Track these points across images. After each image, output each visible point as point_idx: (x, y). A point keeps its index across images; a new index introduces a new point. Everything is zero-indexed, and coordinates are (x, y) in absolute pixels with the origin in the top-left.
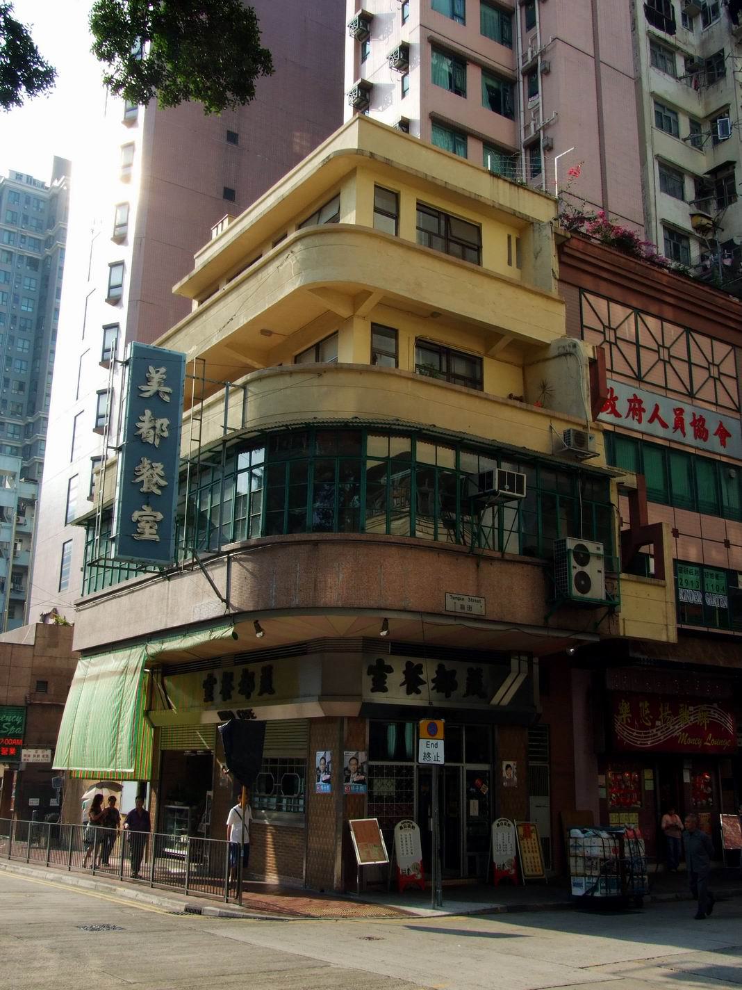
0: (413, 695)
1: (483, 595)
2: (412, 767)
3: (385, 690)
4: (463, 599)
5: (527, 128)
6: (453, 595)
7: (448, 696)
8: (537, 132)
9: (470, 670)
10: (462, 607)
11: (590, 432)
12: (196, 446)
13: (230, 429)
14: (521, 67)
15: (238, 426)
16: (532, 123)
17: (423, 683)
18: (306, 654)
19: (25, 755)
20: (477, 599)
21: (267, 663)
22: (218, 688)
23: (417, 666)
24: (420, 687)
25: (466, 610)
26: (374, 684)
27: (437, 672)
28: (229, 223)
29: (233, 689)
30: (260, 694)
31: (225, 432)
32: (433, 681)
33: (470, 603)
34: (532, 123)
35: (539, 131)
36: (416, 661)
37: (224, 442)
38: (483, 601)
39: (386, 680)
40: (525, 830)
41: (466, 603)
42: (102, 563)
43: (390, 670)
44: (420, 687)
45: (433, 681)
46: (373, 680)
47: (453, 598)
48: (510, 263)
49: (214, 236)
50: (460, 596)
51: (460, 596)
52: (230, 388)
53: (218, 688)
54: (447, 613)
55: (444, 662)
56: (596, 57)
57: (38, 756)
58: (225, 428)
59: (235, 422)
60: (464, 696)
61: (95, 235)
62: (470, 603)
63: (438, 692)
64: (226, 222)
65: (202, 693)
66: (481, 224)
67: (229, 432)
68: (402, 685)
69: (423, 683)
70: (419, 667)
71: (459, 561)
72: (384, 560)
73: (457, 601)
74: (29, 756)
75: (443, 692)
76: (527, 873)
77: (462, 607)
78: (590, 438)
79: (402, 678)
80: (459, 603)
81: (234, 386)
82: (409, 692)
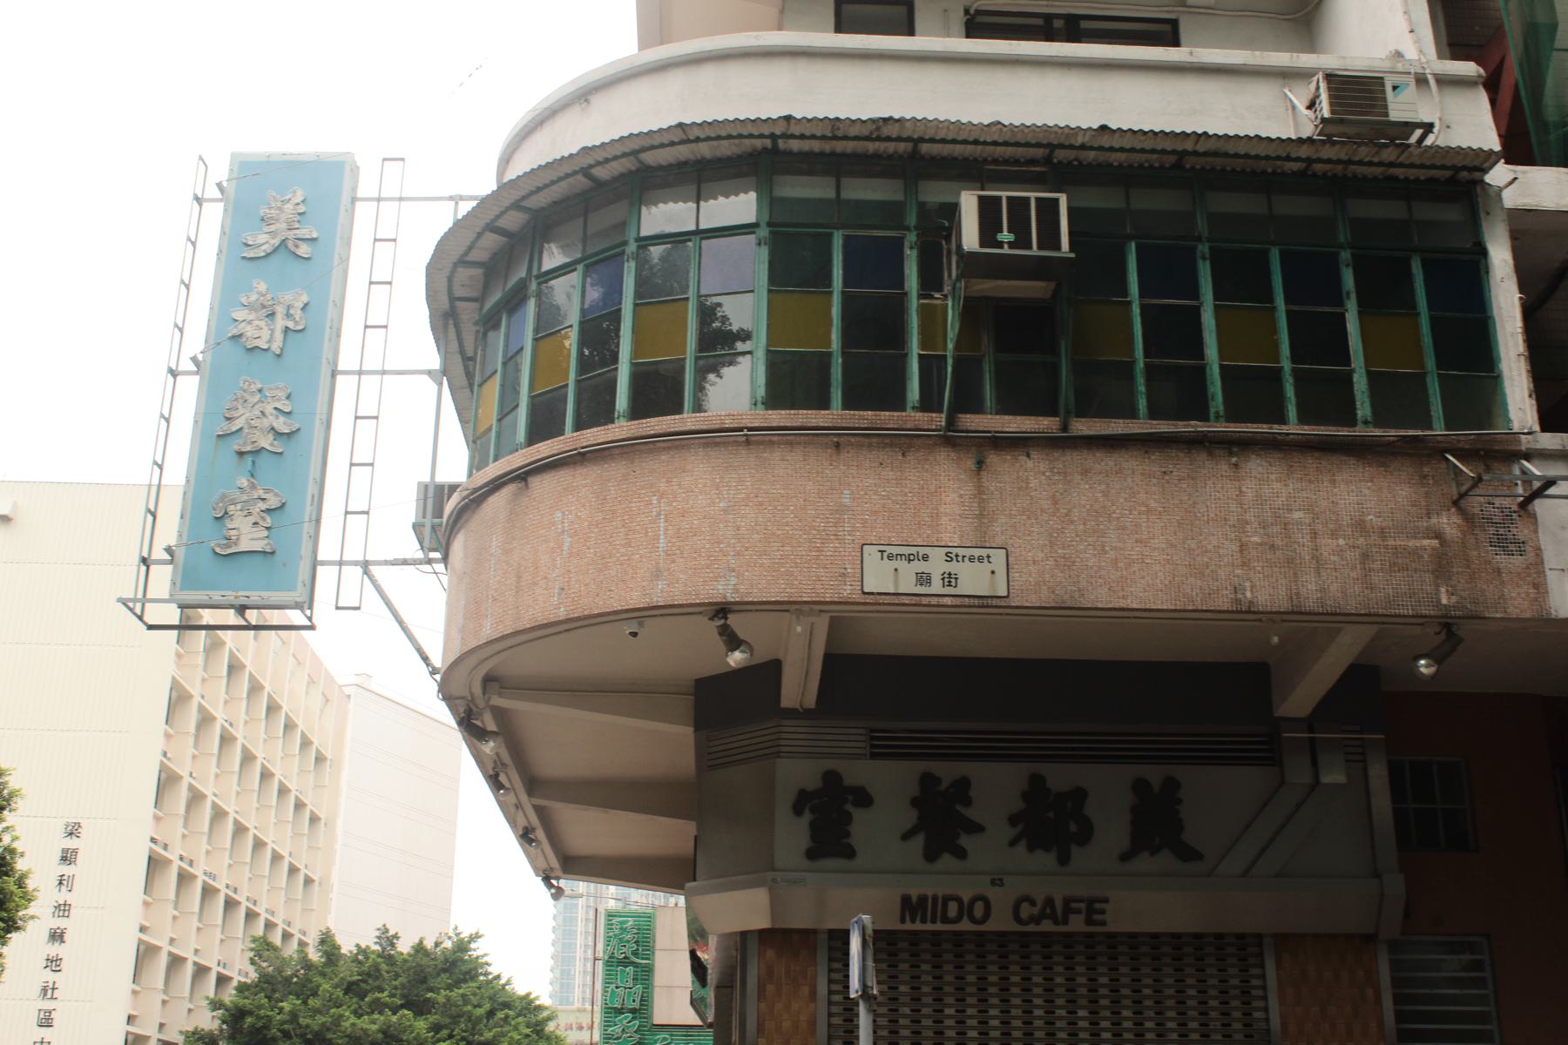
0: (947, 861)
1: (999, 541)
4: (925, 558)
6: (890, 549)
7: (1064, 859)
9: (1140, 786)
10: (924, 579)
17: (976, 828)
20: (977, 552)
24: (965, 841)
25: (936, 587)
26: (813, 837)
32: (1013, 820)
33: (953, 567)
36: (946, 771)
38: (998, 557)
43: (863, 798)
44: (965, 841)
45: (1013, 820)
47: (890, 557)
50: (913, 550)
51: (913, 550)
54: (869, 599)
55: (1043, 768)
60: (1125, 857)
62: (953, 567)
63: (1031, 848)
68: (906, 836)
69: (976, 828)
70: (962, 788)
71: (910, 457)
73: (902, 565)
75: (1047, 850)
77: (924, 579)
78: (1395, 88)
79: (910, 817)
82: (931, 855)
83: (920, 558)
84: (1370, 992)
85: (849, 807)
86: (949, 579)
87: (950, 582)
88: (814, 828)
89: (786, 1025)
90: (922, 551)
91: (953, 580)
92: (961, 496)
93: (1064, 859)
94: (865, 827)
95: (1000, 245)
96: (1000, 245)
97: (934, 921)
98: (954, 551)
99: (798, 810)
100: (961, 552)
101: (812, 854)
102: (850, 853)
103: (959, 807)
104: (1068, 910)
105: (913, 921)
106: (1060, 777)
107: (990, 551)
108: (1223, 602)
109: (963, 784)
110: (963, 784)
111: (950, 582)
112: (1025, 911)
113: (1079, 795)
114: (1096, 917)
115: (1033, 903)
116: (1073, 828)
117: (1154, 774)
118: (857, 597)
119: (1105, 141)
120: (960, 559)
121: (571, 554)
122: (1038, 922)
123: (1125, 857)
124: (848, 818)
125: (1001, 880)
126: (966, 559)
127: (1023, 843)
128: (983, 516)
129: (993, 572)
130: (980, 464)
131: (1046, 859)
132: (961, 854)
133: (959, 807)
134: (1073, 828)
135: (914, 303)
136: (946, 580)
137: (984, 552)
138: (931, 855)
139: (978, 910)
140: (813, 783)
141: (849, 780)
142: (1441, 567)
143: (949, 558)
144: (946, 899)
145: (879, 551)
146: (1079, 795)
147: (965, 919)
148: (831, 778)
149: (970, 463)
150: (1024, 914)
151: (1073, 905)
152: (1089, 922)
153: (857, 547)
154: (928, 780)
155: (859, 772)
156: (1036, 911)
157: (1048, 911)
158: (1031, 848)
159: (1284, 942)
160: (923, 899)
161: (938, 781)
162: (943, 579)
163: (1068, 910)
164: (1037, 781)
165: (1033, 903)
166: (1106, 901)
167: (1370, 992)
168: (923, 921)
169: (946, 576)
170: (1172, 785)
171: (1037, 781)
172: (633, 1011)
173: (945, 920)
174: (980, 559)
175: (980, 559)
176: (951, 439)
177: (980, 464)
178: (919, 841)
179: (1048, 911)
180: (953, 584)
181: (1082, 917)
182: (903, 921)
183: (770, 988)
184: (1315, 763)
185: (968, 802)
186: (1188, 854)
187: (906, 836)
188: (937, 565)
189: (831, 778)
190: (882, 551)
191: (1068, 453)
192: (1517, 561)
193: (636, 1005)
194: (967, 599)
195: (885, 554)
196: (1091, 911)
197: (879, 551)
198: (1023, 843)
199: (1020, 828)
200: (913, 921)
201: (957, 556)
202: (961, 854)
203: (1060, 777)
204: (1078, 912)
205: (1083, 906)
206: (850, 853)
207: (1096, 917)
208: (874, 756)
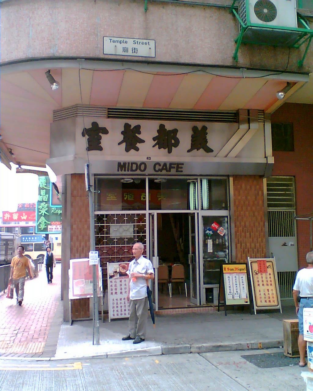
0: (132, 151)
1: (152, 37)
2: (144, 215)
4: (126, 42)
7: (170, 152)
9: (195, 129)
10: (125, 50)
17: (143, 141)
19: (50, 229)
20: (145, 41)
23: (135, 127)
24: (138, 145)
25: (130, 53)
27: (158, 131)
32: (154, 139)
33: (136, 46)
36: (133, 123)
38: (152, 43)
39: (101, 141)
40: (260, 266)
43: (105, 131)
44: (138, 145)
45: (154, 139)
47: (114, 42)
51: (122, 39)
54: (106, 57)
60: (188, 151)
62: (136, 46)
63: (159, 148)
69: (143, 141)
72: (33, 13)
73: (118, 44)
75: (165, 148)
76: (259, 304)
79: (121, 137)
80: (120, 47)
82: (127, 150)
83: (124, 42)
84: (260, 192)
85: (100, 134)
86: (135, 50)
87: (135, 51)
88: (89, 141)
90: (125, 40)
91: (136, 51)
92: (139, 21)
93: (170, 152)
94: (105, 140)
97: (128, 171)
98: (136, 40)
99: (83, 135)
100: (139, 41)
101: (89, 149)
102: (101, 149)
103: (137, 135)
104: (171, 167)
105: (122, 171)
106: (169, 125)
107: (149, 41)
109: (138, 128)
110: (138, 128)
111: (135, 51)
112: (157, 167)
113: (175, 131)
114: (179, 169)
115: (160, 165)
116: (173, 142)
117: (199, 125)
120: (138, 43)
122: (161, 171)
123: (188, 151)
124: (100, 138)
125: (150, 158)
126: (141, 43)
127: (157, 146)
128: (147, 28)
129: (150, 48)
130: (146, 10)
131: (164, 151)
132: (137, 149)
133: (137, 135)
134: (173, 142)
136: (133, 50)
137: (147, 41)
138: (127, 150)
139: (143, 167)
140: (89, 126)
141: (100, 125)
144: (132, 164)
145: (110, 39)
146: (175, 131)
147: (138, 170)
148: (95, 124)
149: (142, 9)
150: (157, 169)
151: (172, 166)
152: (177, 171)
154: (127, 126)
155: (103, 122)
156: (161, 168)
157: (164, 168)
158: (159, 148)
159: (236, 177)
160: (125, 164)
161: (130, 126)
162: (132, 50)
163: (171, 167)
164: (162, 127)
165: (160, 165)
166: (183, 164)
167: (260, 192)
168: (125, 171)
169: (134, 49)
170: (205, 128)
171: (162, 127)
172: (46, 202)
173: (132, 170)
174: (146, 44)
175: (146, 44)
177: (146, 10)
178: (124, 145)
179: (164, 168)
180: (136, 52)
181: (175, 170)
182: (118, 171)
184: (249, 123)
185: (140, 133)
186: (209, 150)
187: (119, 144)
188: (130, 44)
189: (95, 124)
190: (111, 40)
191: (177, 7)
193: (47, 200)
194: (141, 57)
195: (112, 40)
196: (178, 167)
197: (110, 39)
198: (157, 146)
199: (156, 142)
200: (122, 171)
201: (137, 42)
202: (137, 149)
203: (169, 125)
204: (174, 168)
205: (176, 166)
206: (101, 149)
207: (179, 169)
208: (109, 117)
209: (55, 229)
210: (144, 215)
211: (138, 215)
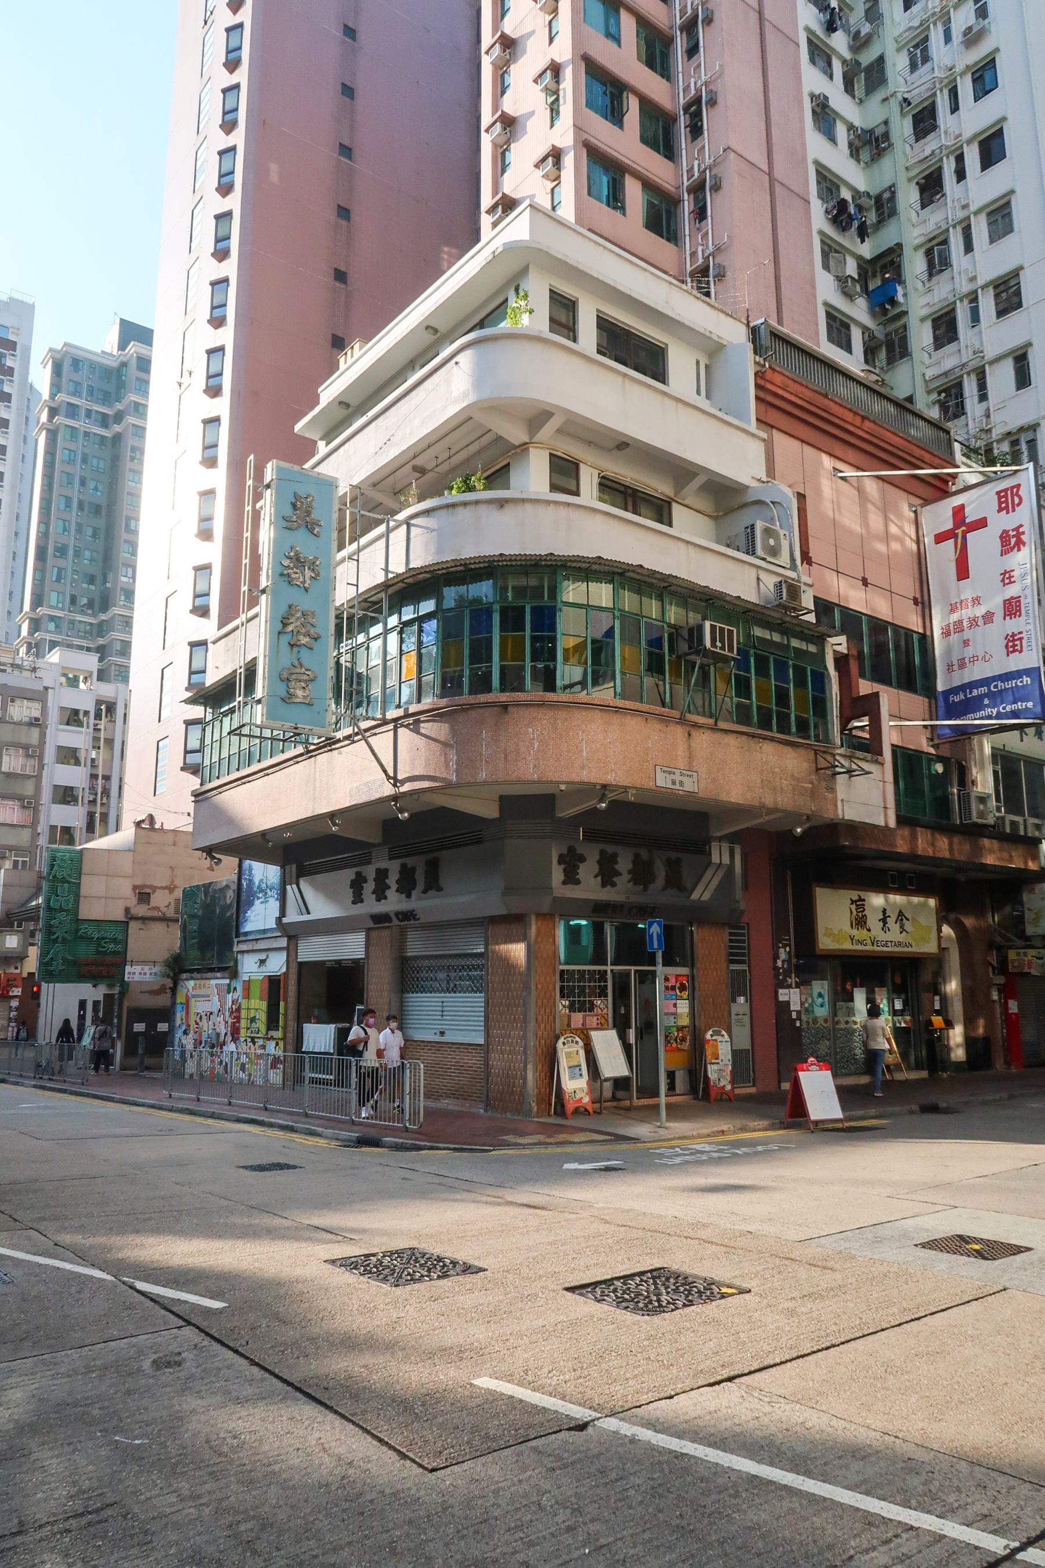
2: (606, 971)
3: (578, 882)
5: (693, 254)
8: (706, 259)
11: (803, 588)
12: (352, 592)
13: (392, 572)
14: (686, 184)
15: (401, 569)
16: (700, 248)
18: (481, 842)
19: (129, 973)
20: (690, 773)
21: (430, 856)
22: (369, 887)
24: (615, 879)
25: (677, 787)
26: (565, 876)
28: (361, 348)
29: (389, 887)
30: (425, 892)
31: (386, 575)
32: (630, 872)
34: (700, 248)
35: (708, 257)
36: (610, 849)
37: (385, 586)
41: (677, 778)
42: (246, 731)
43: (582, 859)
44: (615, 879)
45: (630, 872)
46: (565, 870)
48: (698, 393)
49: (342, 366)
52: (392, 524)
53: (369, 887)
56: (770, 174)
57: (145, 974)
58: (386, 570)
59: (398, 567)
60: (663, 890)
61: (183, 387)
63: (635, 884)
64: (357, 347)
65: (350, 893)
66: (667, 345)
67: (390, 576)
68: (596, 877)
73: (666, 775)
74: (134, 973)
79: (596, 869)
81: (395, 521)
82: (604, 885)
86: (681, 783)
89: (545, 955)
95: (716, 647)
96: (716, 647)
108: (756, 803)
118: (654, 787)
119: (738, 603)
121: (538, 751)
135: (667, 658)
138: (604, 885)
142: (813, 794)
143: (682, 775)
153: (651, 767)
158: (635, 884)
176: (682, 721)
183: (539, 939)
187: (596, 877)
192: (831, 796)
209: (140, 974)
210: (606, 971)
211: (599, 971)
